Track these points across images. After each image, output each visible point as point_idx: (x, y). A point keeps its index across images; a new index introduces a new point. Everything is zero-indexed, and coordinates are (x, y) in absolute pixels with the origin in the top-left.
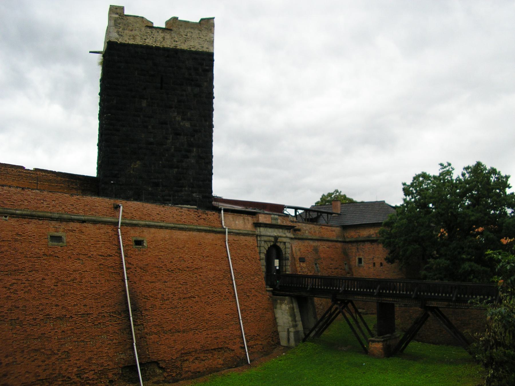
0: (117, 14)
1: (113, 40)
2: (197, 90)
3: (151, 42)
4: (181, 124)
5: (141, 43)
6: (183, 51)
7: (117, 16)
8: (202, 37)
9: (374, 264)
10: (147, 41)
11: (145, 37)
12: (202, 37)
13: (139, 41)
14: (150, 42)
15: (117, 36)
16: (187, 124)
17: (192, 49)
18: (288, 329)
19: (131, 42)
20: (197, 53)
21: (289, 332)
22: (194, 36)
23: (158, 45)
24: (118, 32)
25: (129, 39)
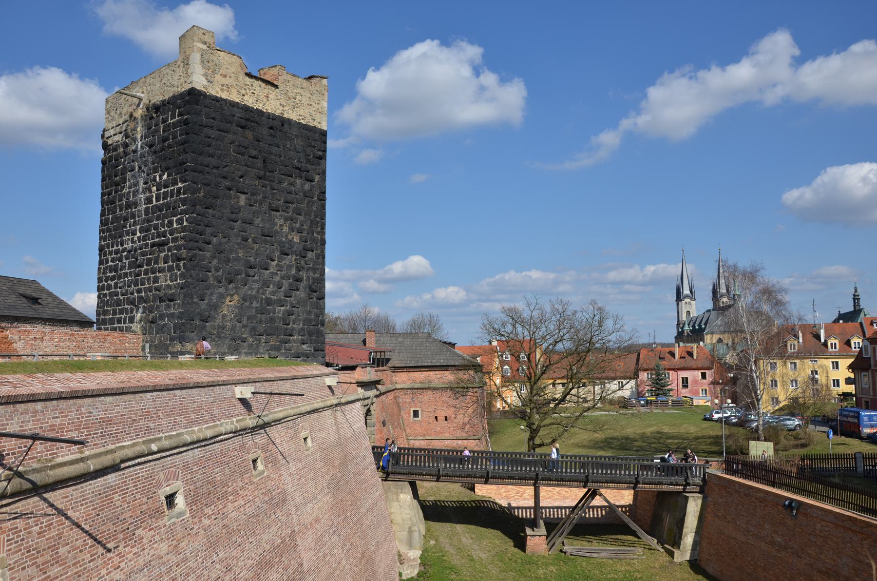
0: (205, 43)
1: (199, 87)
2: (307, 186)
3: (251, 102)
4: (289, 237)
5: (237, 101)
6: (289, 121)
7: (205, 47)
8: (314, 104)
9: (436, 418)
10: (246, 98)
11: (243, 92)
12: (314, 104)
13: (235, 97)
14: (249, 101)
15: (205, 82)
16: (296, 238)
17: (302, 121)
18: (410, 528)
19: (224, 96)
20: (306, 127)
21: (410, 531)
22: (305, 101)
23: (260, 108)
24: (205, 75)
25: (222, 90)
